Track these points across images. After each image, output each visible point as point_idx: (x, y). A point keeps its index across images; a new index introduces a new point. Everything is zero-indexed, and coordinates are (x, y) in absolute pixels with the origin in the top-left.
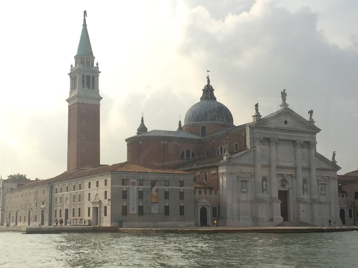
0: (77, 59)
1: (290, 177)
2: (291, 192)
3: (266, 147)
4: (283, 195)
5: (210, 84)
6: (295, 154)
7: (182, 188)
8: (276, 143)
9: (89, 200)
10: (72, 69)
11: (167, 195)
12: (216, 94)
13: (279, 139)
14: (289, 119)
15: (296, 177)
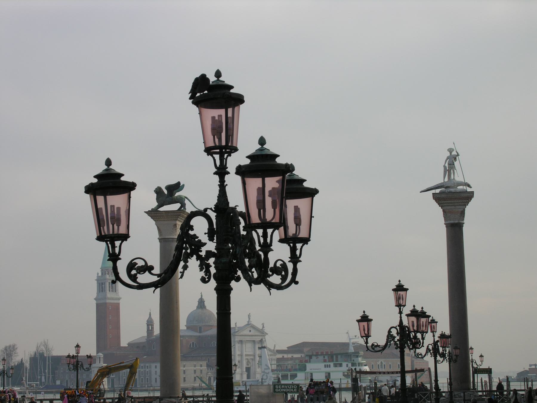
0: (104, 270)
1: (251, 360)
2: (252, 368)
3: (240, 345)
4: (248, 370)
5: (203, 297)
6: (254, 347)
7: (201, 368)
8: (245, 342)
9: (156, 374)
10: (97, 276)
11: (195, 371)
12: (206, 304)
13: (247, 340)
14: (251, 329)
15: (254, 360)
